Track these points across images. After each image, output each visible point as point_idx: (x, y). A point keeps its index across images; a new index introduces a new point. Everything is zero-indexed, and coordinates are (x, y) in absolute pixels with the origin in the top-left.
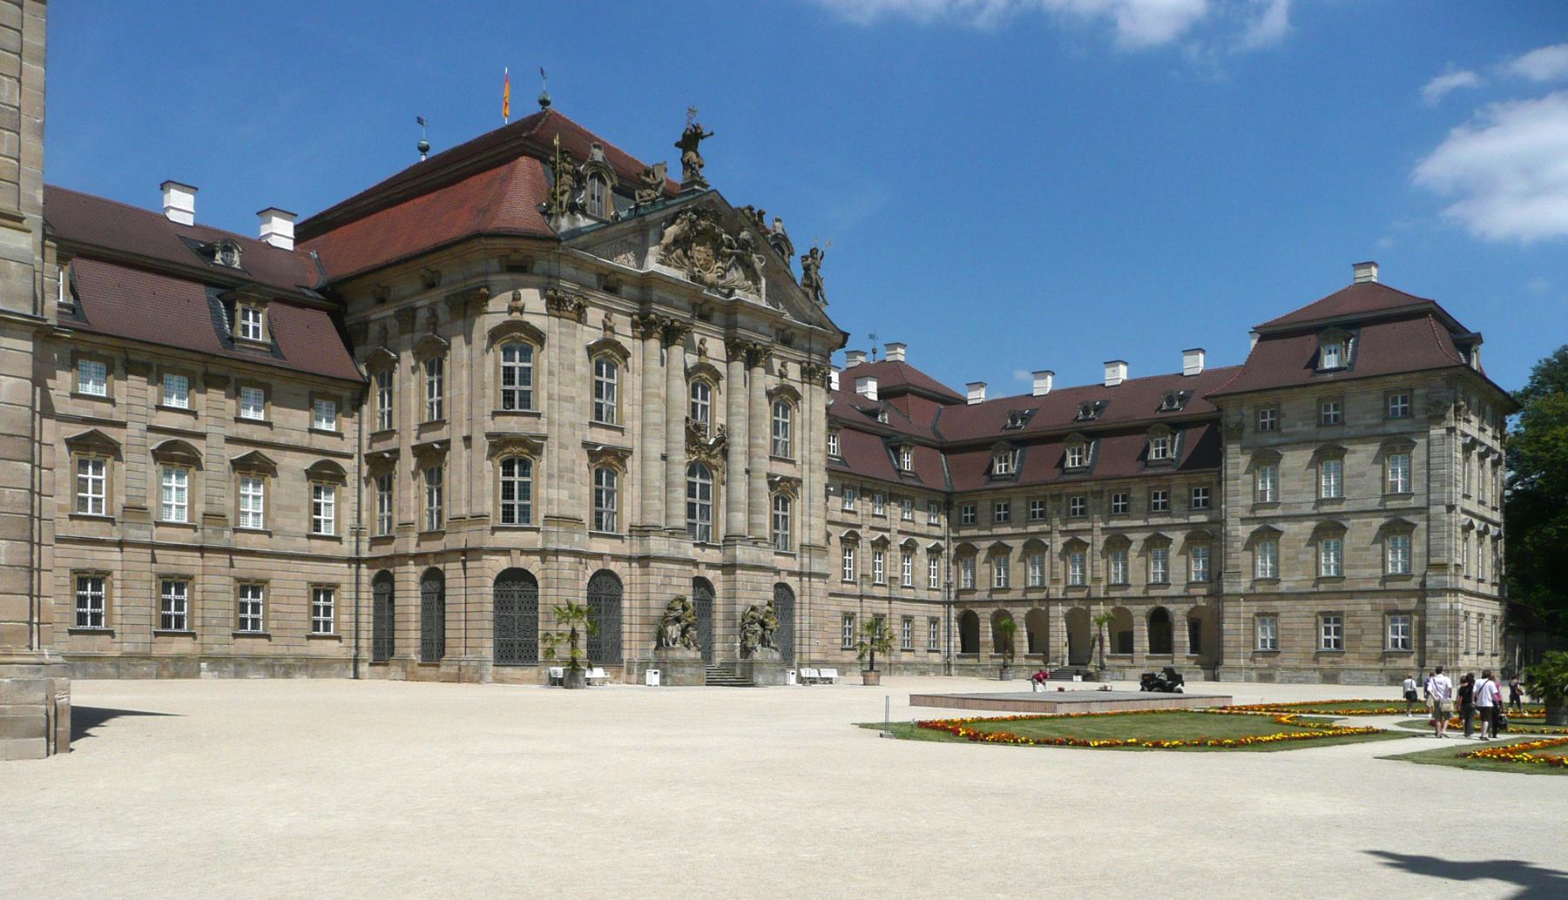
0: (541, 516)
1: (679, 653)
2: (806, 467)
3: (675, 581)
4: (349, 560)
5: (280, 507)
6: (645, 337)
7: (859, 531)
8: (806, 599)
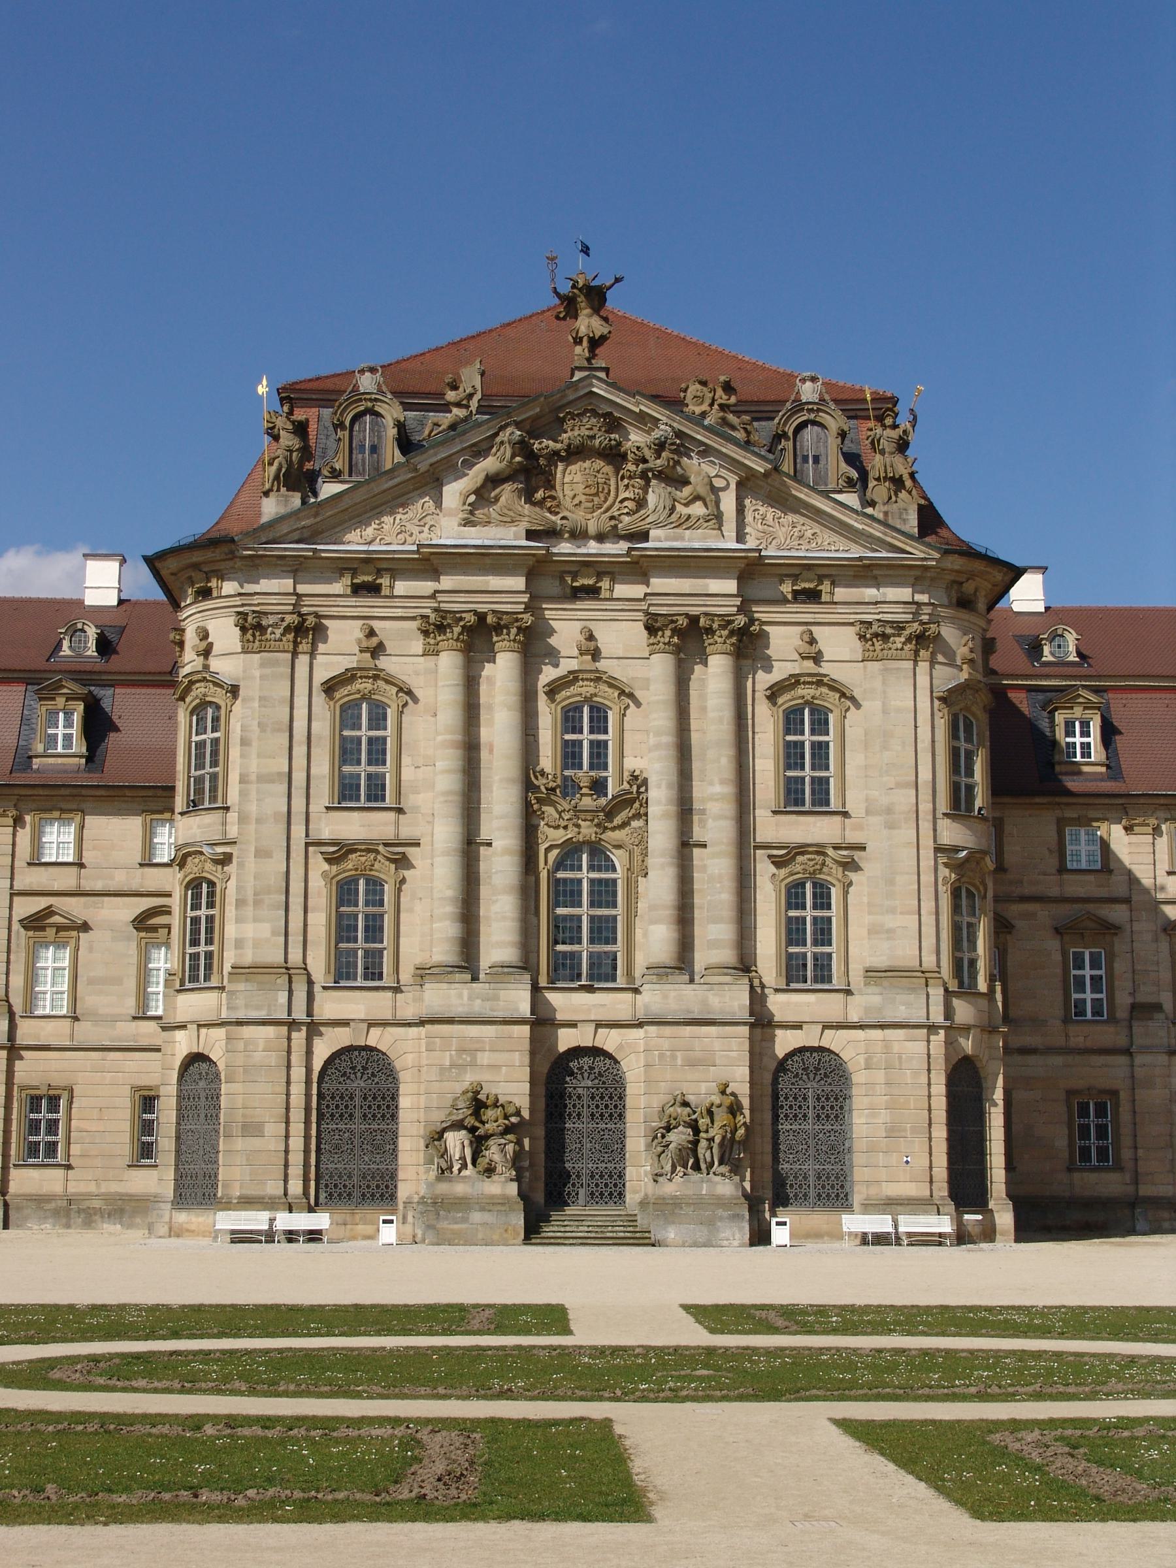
0: (227, 968)
1: (468, 1183)
3: (484, 1058)
5: (91, 981)
6: (431, 652)
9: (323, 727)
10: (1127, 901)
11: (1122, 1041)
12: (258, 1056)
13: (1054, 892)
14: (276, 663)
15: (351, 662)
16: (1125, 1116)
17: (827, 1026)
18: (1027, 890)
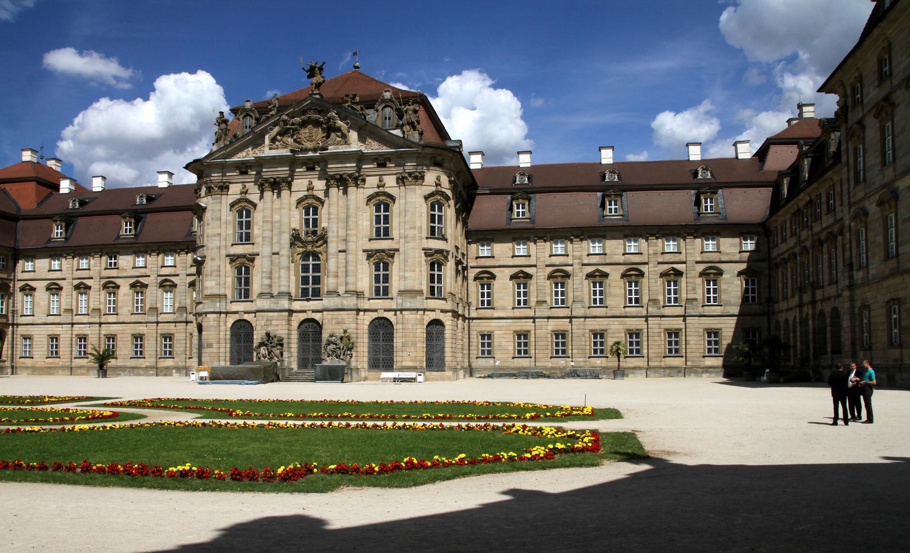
2: (402, 240)
3: (274, 322)
4: (473, 319)
7: (644, 268)
8: (400, 326)
9: (230, 218)
10: (535, 266)
11: (532, 314)
12: (211, 323)
13: (511, 263)
14: (216, 199)
15: (238, 197)
16: (533, 339)
17: (386, 310)
18: (501, 263)
